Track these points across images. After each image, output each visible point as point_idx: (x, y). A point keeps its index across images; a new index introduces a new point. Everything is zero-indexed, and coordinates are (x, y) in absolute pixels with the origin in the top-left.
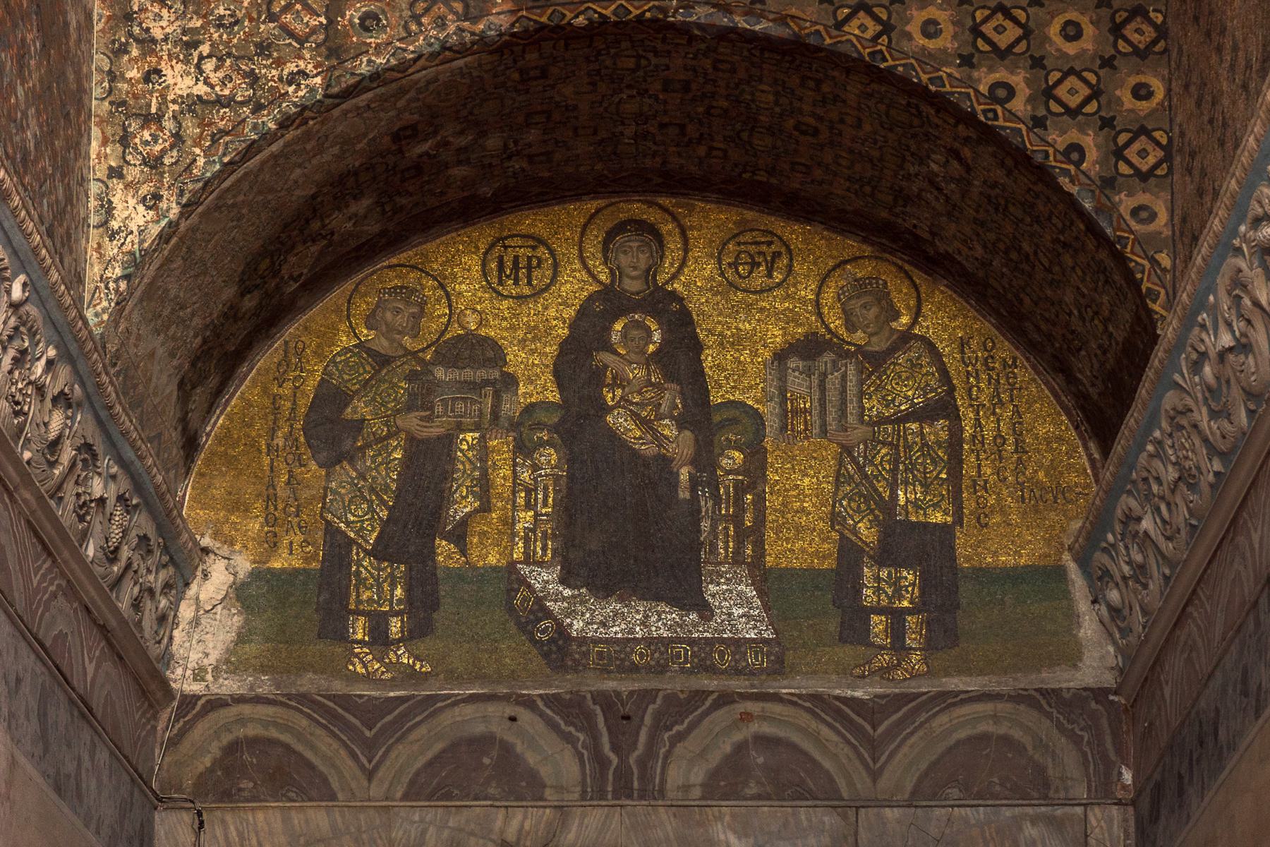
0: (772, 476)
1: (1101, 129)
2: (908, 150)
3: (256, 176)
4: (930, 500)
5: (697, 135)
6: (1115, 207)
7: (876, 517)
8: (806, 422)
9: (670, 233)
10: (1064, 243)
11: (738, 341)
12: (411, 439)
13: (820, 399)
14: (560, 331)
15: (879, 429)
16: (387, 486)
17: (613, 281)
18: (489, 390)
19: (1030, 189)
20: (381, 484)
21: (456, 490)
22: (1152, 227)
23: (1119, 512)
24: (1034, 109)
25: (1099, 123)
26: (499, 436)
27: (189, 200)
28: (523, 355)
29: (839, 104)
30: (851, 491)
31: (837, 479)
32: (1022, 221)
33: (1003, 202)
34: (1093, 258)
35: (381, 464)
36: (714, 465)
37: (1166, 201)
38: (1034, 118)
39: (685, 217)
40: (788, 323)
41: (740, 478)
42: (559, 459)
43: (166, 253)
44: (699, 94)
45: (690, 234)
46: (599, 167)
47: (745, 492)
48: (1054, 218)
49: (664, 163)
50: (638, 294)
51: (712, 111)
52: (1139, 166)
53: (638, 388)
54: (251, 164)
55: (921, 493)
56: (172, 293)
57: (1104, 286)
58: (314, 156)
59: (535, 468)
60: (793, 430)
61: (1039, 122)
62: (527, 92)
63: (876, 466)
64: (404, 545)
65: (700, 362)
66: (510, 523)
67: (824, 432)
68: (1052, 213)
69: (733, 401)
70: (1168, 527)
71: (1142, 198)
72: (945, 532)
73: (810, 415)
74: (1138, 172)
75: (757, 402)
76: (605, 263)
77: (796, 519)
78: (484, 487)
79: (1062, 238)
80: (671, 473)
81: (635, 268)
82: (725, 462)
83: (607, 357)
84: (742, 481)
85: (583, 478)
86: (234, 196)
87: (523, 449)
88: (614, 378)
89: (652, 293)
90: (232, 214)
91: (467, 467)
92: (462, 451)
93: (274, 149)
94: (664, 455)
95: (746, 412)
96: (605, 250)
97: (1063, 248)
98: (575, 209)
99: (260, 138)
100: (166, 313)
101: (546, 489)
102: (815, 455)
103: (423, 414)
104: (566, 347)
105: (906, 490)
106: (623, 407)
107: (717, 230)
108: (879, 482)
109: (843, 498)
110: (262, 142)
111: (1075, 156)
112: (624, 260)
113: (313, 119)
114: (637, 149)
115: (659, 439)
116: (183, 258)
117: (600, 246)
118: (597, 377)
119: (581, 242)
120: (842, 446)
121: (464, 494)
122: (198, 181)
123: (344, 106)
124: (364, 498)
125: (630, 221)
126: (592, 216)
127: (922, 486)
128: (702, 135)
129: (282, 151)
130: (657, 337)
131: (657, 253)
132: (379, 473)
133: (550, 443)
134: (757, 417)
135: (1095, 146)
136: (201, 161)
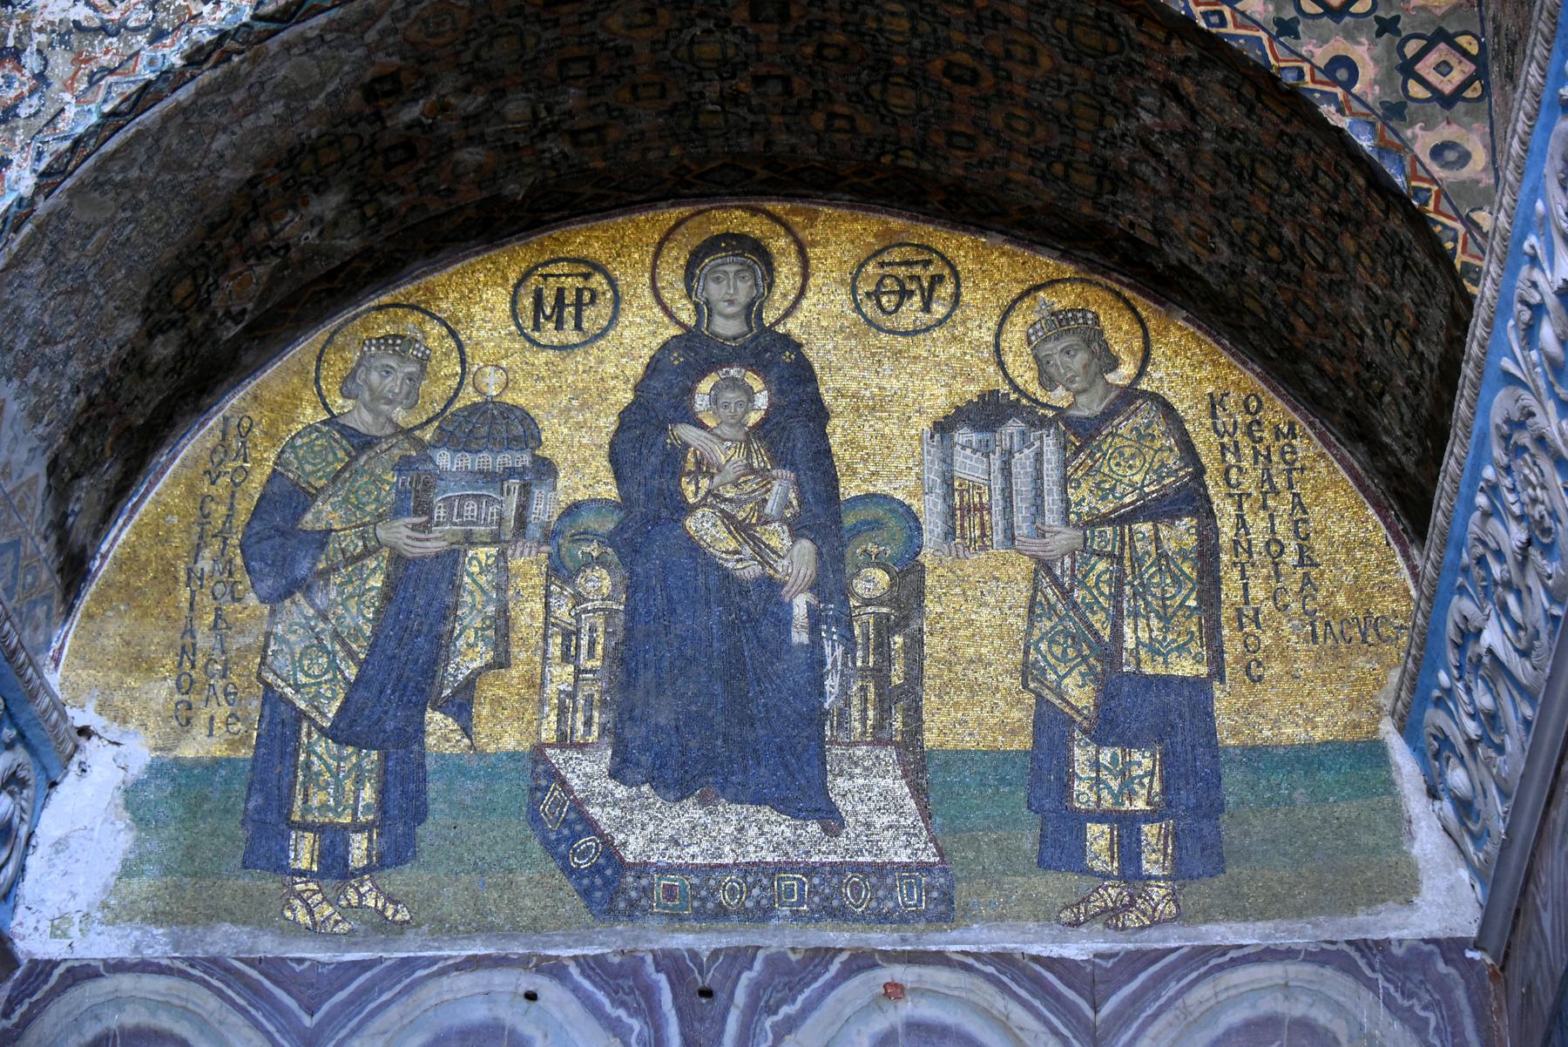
0: (932, 607)
1: (1379, 34)
2: (1107, 95)
3: (157, 141)
4: (1174, 641)
5: (809, 95)
6: (1405, 146)
7: (1091, 668)
8: (982, 525)
9: (782, 252)
10: (1340, 215)
11: (878, 406)
12: (397, 559)
14: (620, 395)
16: (358, 629)
17: (699, 322)
18: (515, 483)
19: (1282, 133)
20: (349, 627)
21: (460, 635)
22: (1466, 173)
23: (1451, 630)
24: (1278, 8)
25: (1376, 27)
26: (526, 551)
27: (50, 166)
28: (566, 431)
29: (1001, 26)
30: (1053, 628)
31: (1031, 611)
32: (1276, 189)
33: (1247, 163)
34: (1382, 232)
35: (351, 596)
36: (845, 592)
37: (1482, 137)
38: (1279, 22)
39: (805, 228)
40: (954, 378)
41: (885, 610)
42: (614, 585)
43: (15, 247)
44: (803, 23)
45: (813, 252)
46: (675, 152)
47: (891, 631)
48: (1321, 175)
49: (769, 144)
50: (735, 338)
51: (826, 52)
52: (1440, 87)
53: (732, 477)
54: (150, 116)
55: (1160, 630)
56: (30, 315)
57: (1402, 275)
58: (246, 115)
59: (579, 598)
60: (963, 537)
61: (1286, 28)
62: (556, 23)
63: (1089, 589)
64: (380, 719)
65: (825, 436)
66: (537, 684)
67: (1010, 538)
68: (1316, 167)
69: (874, 495)
70: (1522, 634)
71: (1446, 133)
72: (1198, 688)
73: (990, 513)
74: (1438, 96)
75: (910, 494)
76: (689, 296)
78: (502, 626)
79: (1336, 207)
80: (780, 603)
81: (731, 302)
82: (860, 586)
83: (687, 432)
84: (887, 616)
85: (649, 613)
86: (123, 169)
87: (560, 571)
88: (699, 463)
89: (755, 337)
90: (122, 199)
91: (478, 598)
92: (470, 575)
93: (182, 98)
94: (771, 578)
95: (893, 511)
96: (689, 277)
97: (1340, 224)
98: (647, 220)
99: (158, 78)
100: (21, 345)
101: (592, 629)
102: (997, 574)
103: (417, 520)
104: (627, 418)
106: (712, 506)
107: (849, 246)
109: (1041, 639)
110: (160, 85)
111: (1342, 74)
112: (716, 291)
113: (239, 53)
114: (726, 121)
115: (762, 552)
116: (45, 259)
117: (681, 272)
118: (673, 461)
119: (654, 267)
120: (1039, 560)
121: (472, 640)
122: (65, 138)
123: (284, 35)
124: (322, 648)
125: (727, 236)
126: (672, 230)
127: (1160, 618)
128: (815, 92)
129: (194, 102)
130: (762, 401)
131: (763, 279)
132: (347, 610)
133: (601, 561)
134: (911, 518)
135: (1372, 58)
136: (71, 112)
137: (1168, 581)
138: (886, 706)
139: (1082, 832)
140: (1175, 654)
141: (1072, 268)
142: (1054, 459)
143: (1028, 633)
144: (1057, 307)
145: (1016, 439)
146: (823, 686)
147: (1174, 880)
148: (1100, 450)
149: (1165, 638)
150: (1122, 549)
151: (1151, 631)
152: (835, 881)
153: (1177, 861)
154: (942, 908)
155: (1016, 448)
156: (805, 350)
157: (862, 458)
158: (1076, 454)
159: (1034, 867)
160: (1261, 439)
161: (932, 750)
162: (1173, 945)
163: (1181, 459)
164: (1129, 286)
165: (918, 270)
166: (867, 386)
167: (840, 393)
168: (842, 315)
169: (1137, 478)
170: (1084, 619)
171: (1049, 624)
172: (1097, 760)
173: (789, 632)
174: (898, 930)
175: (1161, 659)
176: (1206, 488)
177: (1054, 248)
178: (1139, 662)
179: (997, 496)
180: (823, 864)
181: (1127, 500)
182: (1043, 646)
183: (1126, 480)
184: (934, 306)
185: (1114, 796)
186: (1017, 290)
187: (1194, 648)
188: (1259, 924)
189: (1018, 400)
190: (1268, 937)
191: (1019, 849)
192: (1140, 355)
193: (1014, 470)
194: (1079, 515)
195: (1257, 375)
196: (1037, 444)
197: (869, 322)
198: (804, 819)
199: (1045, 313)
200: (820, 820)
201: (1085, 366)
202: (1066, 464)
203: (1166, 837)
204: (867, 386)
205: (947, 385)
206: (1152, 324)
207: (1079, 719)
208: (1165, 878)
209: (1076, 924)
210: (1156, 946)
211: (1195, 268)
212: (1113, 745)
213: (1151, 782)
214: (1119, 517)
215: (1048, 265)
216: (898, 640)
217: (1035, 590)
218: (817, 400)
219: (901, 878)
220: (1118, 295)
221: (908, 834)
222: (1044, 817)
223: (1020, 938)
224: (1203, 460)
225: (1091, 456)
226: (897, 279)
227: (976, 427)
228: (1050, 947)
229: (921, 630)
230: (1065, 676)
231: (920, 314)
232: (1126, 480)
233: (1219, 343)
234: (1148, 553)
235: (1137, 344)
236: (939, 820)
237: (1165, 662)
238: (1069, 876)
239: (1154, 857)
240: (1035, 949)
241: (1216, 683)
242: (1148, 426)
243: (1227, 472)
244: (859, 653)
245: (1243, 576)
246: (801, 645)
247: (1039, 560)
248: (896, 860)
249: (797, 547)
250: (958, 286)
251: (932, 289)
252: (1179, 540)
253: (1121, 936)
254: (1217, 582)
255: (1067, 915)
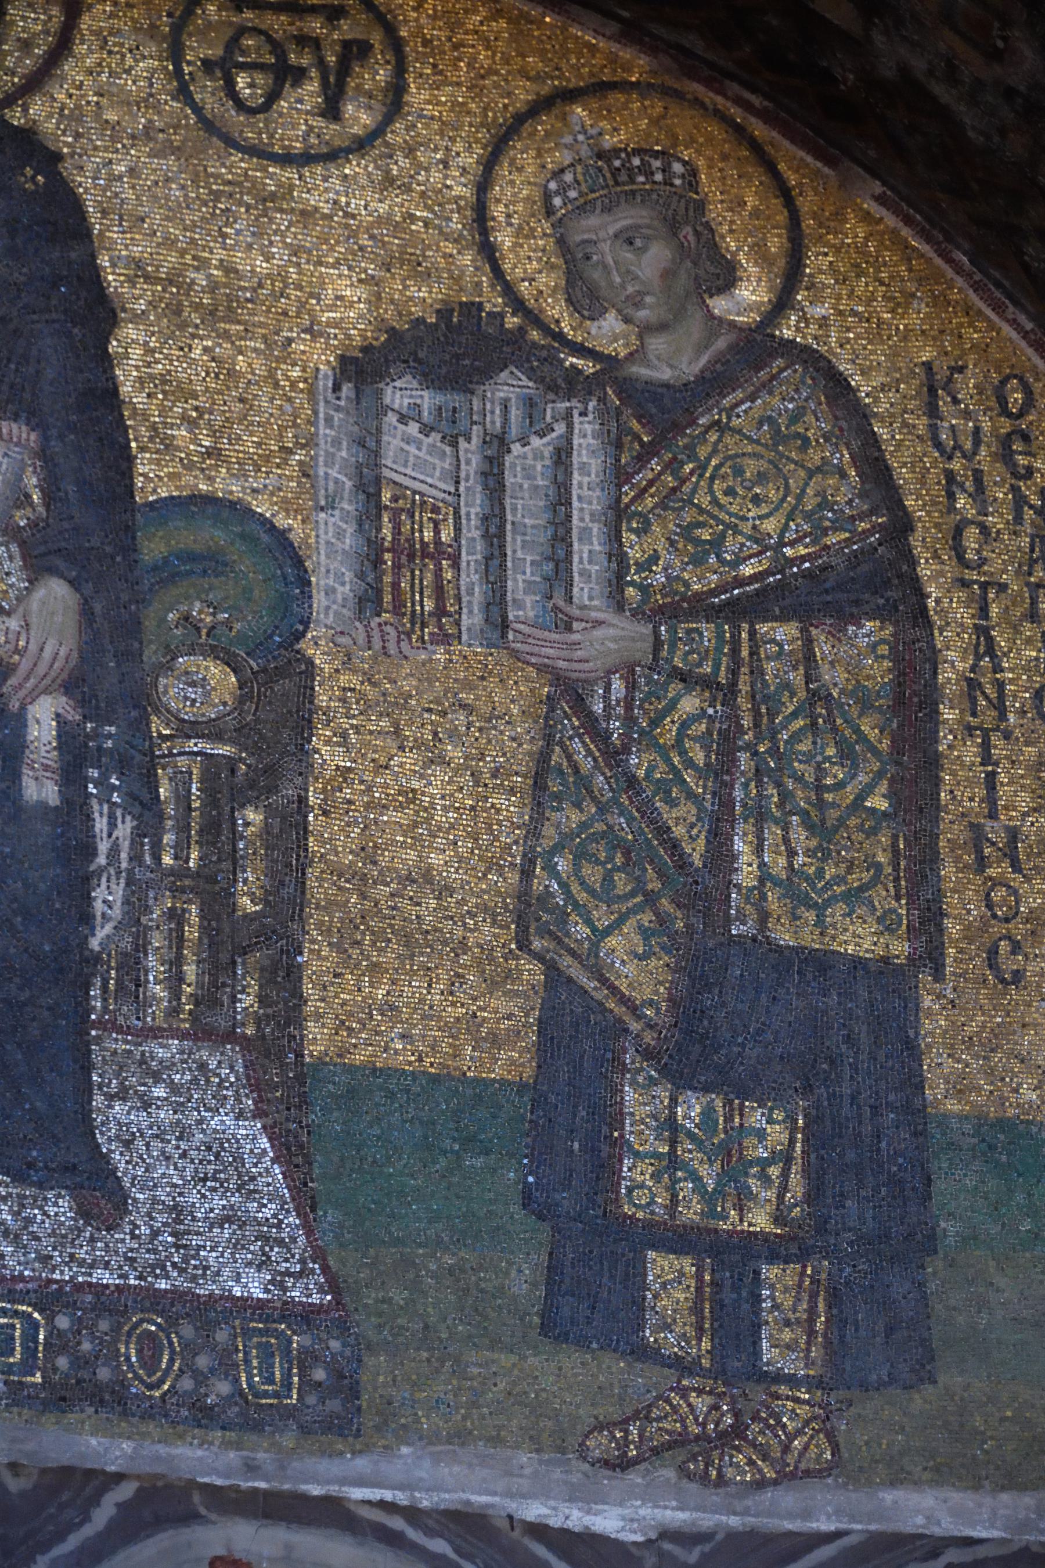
4: (839, 880)
7: (662, 920)
13: (485, 519)
15: (673, 630)
30: (583, 826)
31: (539, 783)
41: (224, 750)
47: (240, 798)
55: (809, 852)
63: (664, 752)
65: (105, 362)
69: (209, 500)
73: (456, 565)
75: (286, 506)
77: (404, 904)
105: (761, 840)
108: (672, 803)
109: (557, 849)
137: (831, 751)
138: (224, 957)
139: (637, 1271)
140: (841, 908)
141: (643, 61)
142: (595, 465)
143: (533, 832)
144: (609, 141)
145: (514, 413)
146: (89, 900)
147: (828, 1389)
148: (692, 456)
149: (820, 873)
150: (734, 673)
151: (792, 853)
152: (104, 1325)
153: (836, 1350)
154: (334, 1405)
155: (514, 431)
156: (66, 168)
157: (184, 418)
158: (642, 460)
159: (534, 1334)
160: (1030, 471)
161: (320, 1062)
162: (826, 1526)
163: (863, 495)
164: (763, 115)
165: (316, 26)
166: (202, 264)
167: (138, 271)
168: (148, 101)
169: (770, 526)
170: (647, 811)
171: (575, 817)
172: (673, 1115)
173: (16, 777)
174: (238, 1446)
175: (811, 916)
176: (913, 563)
177: (609, 15)
178: (764, 917)
179: (472, 531)
180: (79, 1288)
181: (747, 570)
182: (562, 865)
183: (746, 528)
184: (349, 109)
185: (709, 1199)
186: (523, 94)
187: (882, 898)
188: (1005, 1497)
189: (521, 330)
190: (1024, 1526)
191: (501, 1290)
192: (782, 263)
193: (509, 480)
194: (644, 589)
195: (1025, 335)
196: (560, 428)
197: (208, 125)
198: (40, 1185)
199: (585, 151)
200: (74, 1190)
201: (668, 275)
202: (620, 476)
203: (813, 1297)
204: (202, 264)
205: (370, 281)
206: (806, 203)
207: (635, 1026)
208: (811, 1384)
209: (622, 1464)
210: (789, 1526)
211: (940, 91)
212: (706, 1089)
213: (785, 1175)
214: (728, 603)
215: (593, 49)
216: (254, 816)
217: (549, 739)
218: (94, 278)
219: (247, 1333)
220: (739, 131)
221: (266, 1239)
222: (556, 1229)
223: (500, 1486)
224: (909, 502)
225: (673, 466)
226: (270, 39)
227: (430, 379)
228: (565, 1508)
229: (302, 800)
230: (608, 932)
231: (318, 122)
232: (746, 528)
233: (949, 261)
234: (787, 686)
235: (775, 244)
236: (332, 1216)
237: (820, 922)
238: (607, 1359)
239: (787, 1335)
240: (534, 1511)
241: (925, 978)
242: (795, 418)
243: (958, 532)
244: (168, 838)
245: (986, 759)
246: (43, 805)
247: (558, 679)
248: (237, 1292)
249: (40, 593)
250: (400, 69)
251: (344, 70)
252: (854, 669)
253: (715, 1497)
254: (932, 763)
255: (599, 1444)
